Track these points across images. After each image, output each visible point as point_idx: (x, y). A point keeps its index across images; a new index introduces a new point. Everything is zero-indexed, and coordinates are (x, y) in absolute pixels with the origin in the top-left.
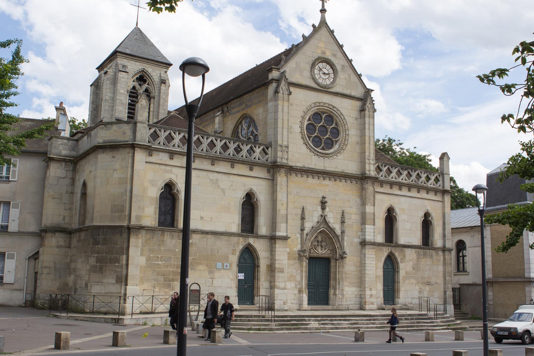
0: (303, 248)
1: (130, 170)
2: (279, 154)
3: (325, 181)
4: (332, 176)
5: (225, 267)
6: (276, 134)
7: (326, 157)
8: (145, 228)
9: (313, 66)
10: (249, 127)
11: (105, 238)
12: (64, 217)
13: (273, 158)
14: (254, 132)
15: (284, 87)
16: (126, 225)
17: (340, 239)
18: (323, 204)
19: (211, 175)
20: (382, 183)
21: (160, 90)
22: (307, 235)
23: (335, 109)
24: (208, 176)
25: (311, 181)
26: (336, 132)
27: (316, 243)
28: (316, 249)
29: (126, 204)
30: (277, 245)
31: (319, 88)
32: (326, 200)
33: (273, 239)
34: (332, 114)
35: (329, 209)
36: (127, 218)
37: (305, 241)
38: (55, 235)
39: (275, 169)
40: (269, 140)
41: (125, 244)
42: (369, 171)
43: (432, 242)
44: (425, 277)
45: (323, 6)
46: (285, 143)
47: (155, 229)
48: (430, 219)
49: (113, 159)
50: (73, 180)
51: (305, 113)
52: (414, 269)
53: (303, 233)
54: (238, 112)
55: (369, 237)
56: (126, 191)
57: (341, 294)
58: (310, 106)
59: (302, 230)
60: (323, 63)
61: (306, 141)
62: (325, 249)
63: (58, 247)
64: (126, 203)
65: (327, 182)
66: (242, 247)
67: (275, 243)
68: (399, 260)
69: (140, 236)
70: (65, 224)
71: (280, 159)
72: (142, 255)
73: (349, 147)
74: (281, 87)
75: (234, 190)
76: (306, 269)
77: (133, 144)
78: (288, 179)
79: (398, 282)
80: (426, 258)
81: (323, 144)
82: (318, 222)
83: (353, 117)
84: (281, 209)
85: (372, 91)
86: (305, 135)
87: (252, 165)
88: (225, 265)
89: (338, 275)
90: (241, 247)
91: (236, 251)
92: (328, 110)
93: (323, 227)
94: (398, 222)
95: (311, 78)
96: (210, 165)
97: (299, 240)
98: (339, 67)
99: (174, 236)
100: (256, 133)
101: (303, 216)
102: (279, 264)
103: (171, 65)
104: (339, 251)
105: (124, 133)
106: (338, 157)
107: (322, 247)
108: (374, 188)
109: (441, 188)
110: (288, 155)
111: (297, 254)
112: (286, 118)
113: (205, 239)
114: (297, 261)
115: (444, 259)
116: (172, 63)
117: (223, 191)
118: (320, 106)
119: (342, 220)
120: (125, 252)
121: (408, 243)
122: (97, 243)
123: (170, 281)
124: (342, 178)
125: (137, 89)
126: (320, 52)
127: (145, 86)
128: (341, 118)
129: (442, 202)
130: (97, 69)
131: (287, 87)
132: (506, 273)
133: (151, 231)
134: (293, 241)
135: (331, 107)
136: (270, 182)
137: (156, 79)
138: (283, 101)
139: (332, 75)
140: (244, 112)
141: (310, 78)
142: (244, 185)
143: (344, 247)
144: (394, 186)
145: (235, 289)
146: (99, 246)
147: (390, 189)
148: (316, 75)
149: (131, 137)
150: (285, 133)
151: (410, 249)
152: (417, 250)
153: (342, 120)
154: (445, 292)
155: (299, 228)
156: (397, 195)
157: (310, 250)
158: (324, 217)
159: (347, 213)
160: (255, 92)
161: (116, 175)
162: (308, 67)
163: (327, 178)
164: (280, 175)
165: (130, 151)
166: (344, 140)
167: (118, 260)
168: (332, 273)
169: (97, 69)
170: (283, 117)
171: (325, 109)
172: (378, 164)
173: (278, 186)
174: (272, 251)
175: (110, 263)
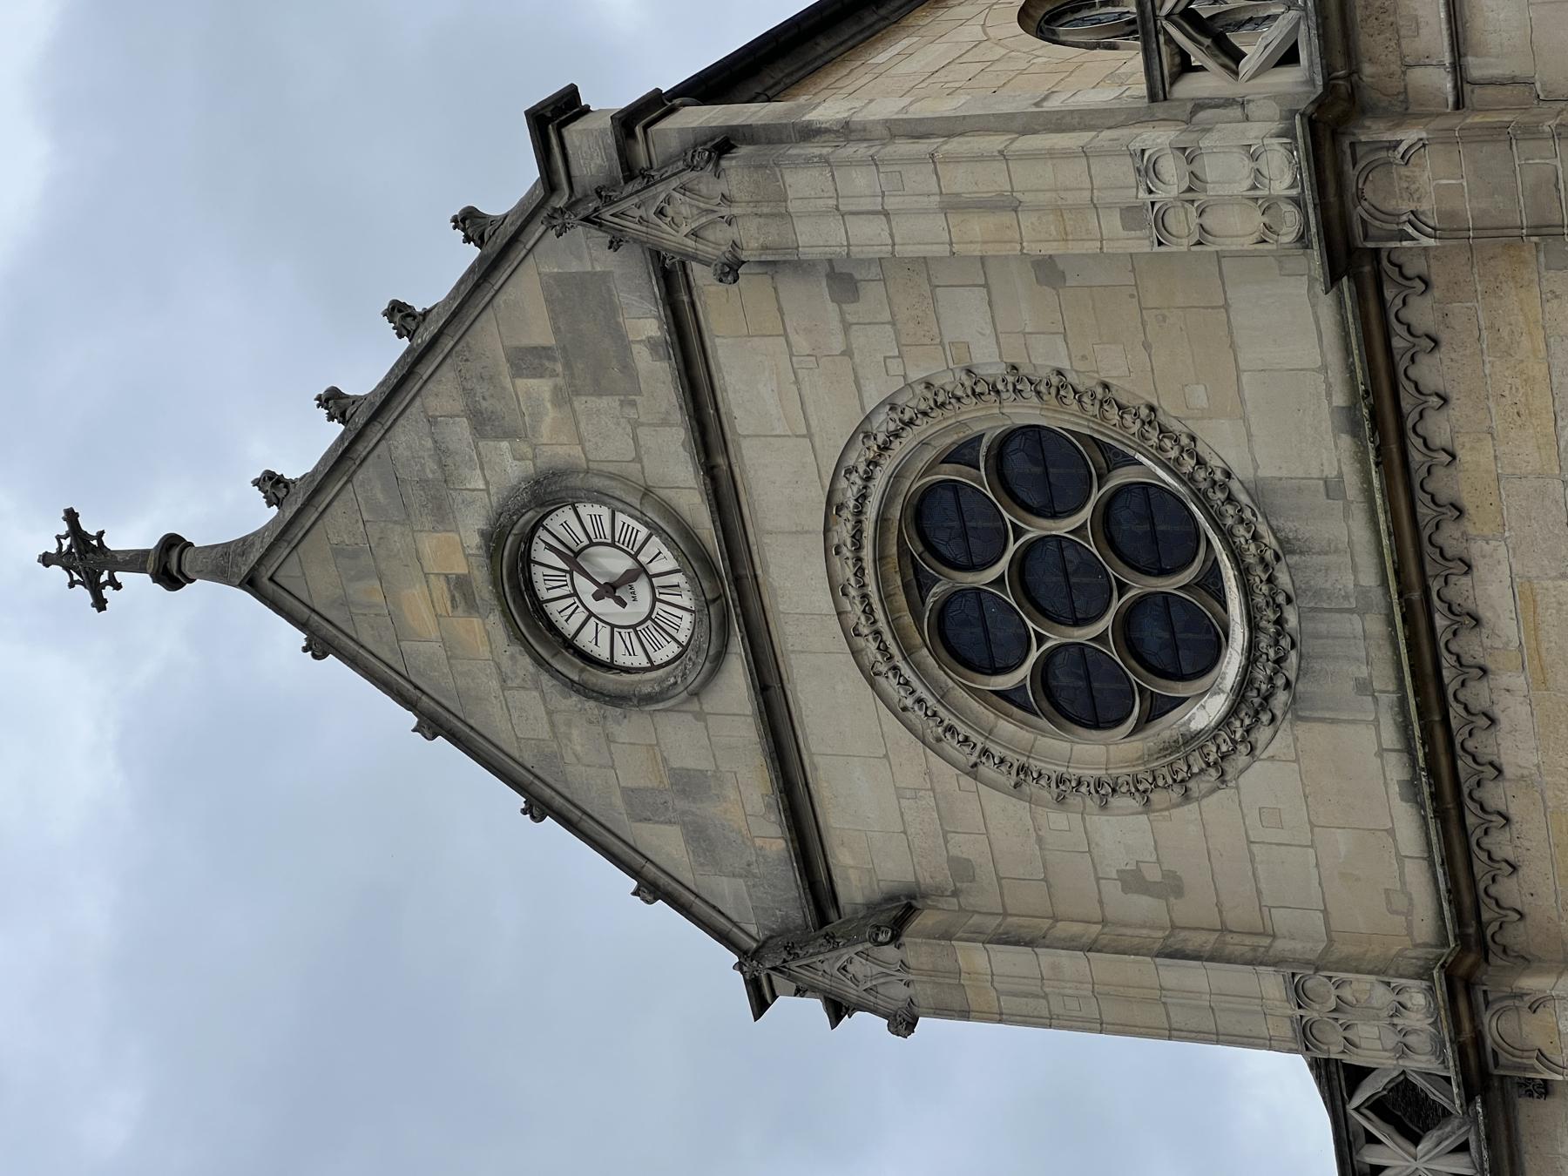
3: (1485, 613)
31: (737, 645)
34: (896, 512)
60: (544, 594)
83: (846, 327)
92: (880, 558)
95: (695, 706)
126: (476, 622)
135: (843, 532)
139: (596, 519)
141: (700, 716)
162: (630, 728)
171: (882, 581)
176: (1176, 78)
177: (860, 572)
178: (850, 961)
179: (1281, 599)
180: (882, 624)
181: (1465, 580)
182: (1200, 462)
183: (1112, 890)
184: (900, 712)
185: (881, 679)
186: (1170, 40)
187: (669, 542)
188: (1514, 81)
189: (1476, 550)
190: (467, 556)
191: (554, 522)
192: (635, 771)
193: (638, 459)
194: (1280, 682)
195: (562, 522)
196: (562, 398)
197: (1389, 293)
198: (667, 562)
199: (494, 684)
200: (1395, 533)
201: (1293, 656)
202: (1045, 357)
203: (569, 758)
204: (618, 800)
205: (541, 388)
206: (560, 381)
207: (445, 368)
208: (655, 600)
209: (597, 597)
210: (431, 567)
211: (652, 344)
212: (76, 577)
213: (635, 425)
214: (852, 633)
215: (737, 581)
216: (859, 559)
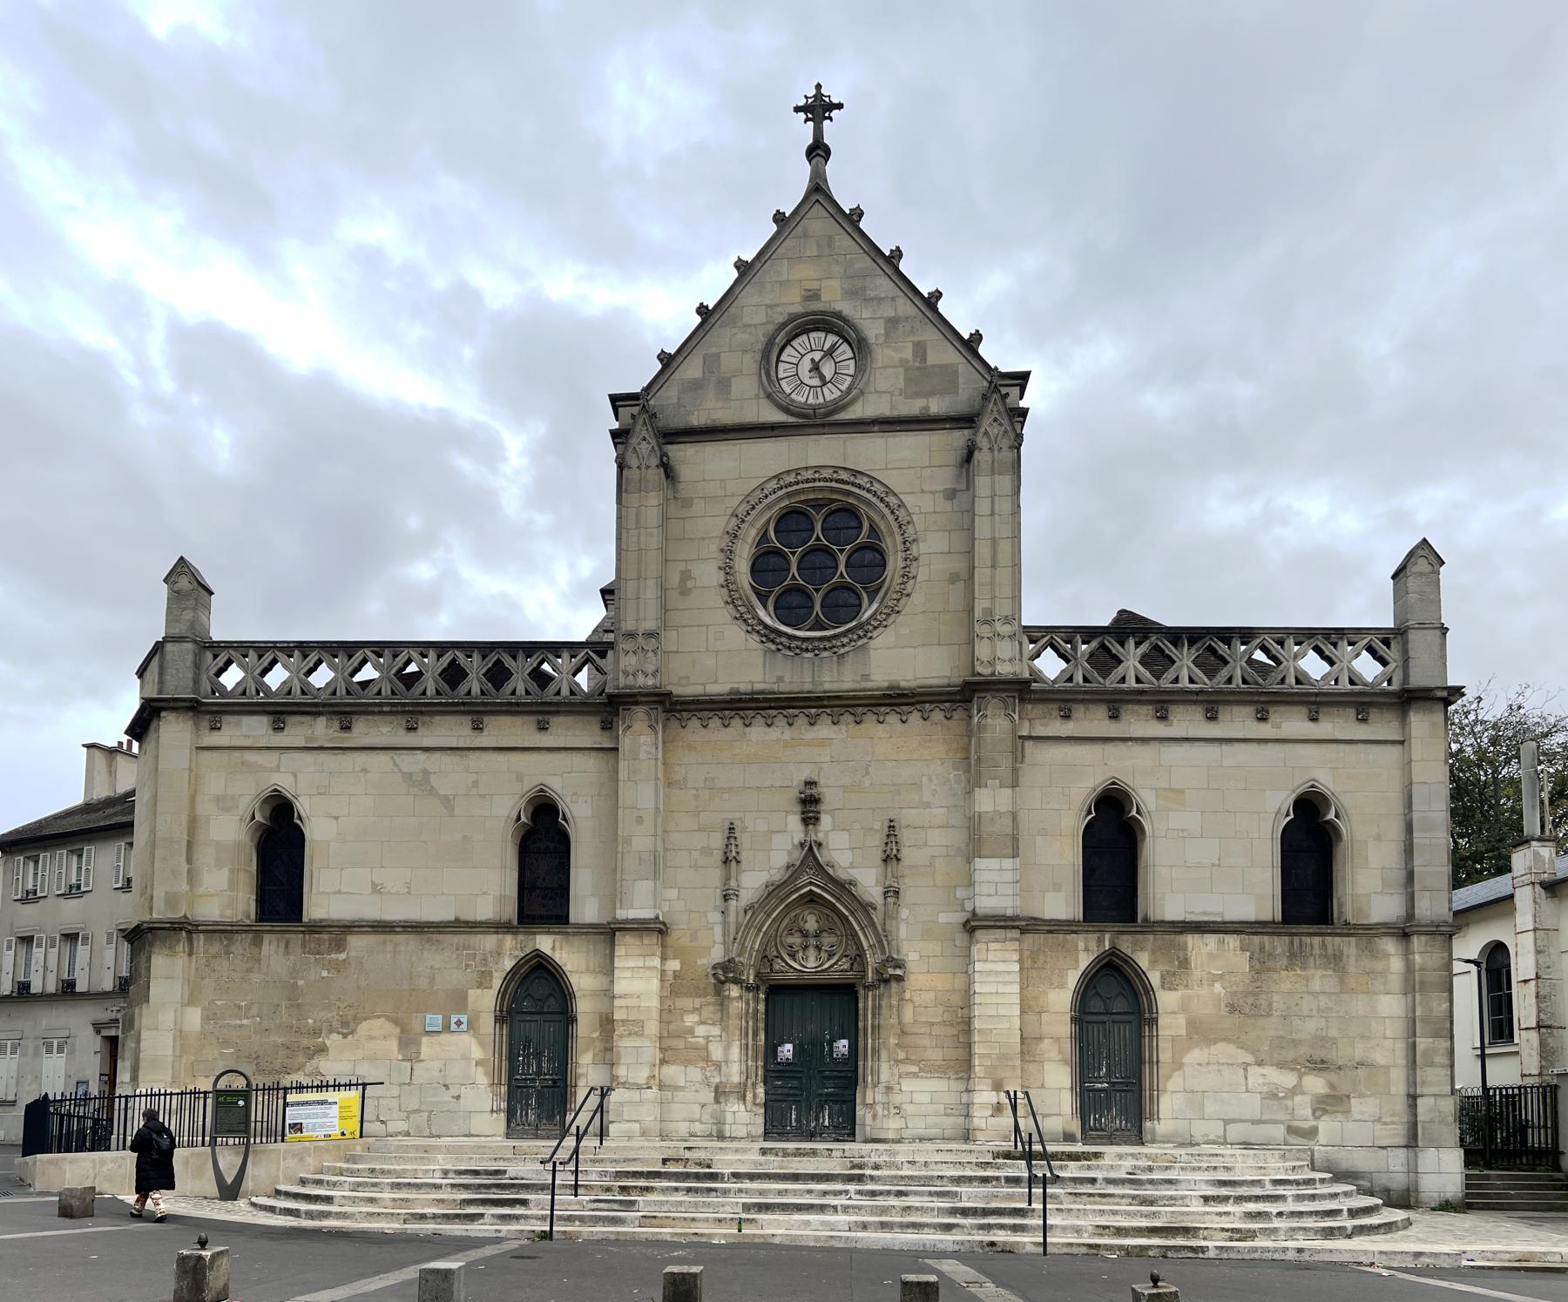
3: (815, 728)
4: (843, 710)
5: (453, 1027)
7: (825, 649)
8: (200, 928)
9: (770, 353)
18: (810, 805)
19: (407, 762)
23: (862, 481)
24: (396, 764)
25: (761, 735)
26: (871, 560)
28: (793, 956)
31: (792, 419)
34: (851, 500)
35: (834, 821)
48: (1331, 816)
52: (1233, 1008)
60: (812, 335)
62: (830, 956)
65: (824, 730)
66: (513, 963)
68: (1154, 978)
71: (631, 677)
73: (917, 600)
75: (484, 796)
80: (1303, 968)
82: (788, 867)
83: (933, 493)
90: (509, 964)
91: (491, 977)
92: (832, 490)
93: (811, 883)
95: (762, 395)
96: (402, 732)
97: (718, 930)
99: (291, 946)
104: (872, 960)
107: (818, 948)
111: (710, 976)
113: (389, 948)
114: (711, 999)
115: (1409, 968)
117: (447, 801)
119: (885, 851)
121: (1205, 913)
126: (799, 300)
129: (1402, 742)
133: (223, 936)
135: (844, 476)
141: (757, 397)
142: (520, 778)
144: (1125, 707)
147: (1107, 721)
148: (783, 383)
151: (1212, 940)
152: (1256, 939)
153: (893, 513)
156: (1145, 740)
158: (811, 848)
162: (750, 363)
163: (824, 716)
164: (629, 727)
171: (821, 489)
176: (1029, 637)
177: (826, 480)
178: (649, 443)
179: (817, 652)
180: (801, 486)
181: (830, 722)
182: (875, 628)
183: (682, 566)
184: (761, 487)
185: (776, 481)
186: (1043, 637)
187: (841, 398)
188: (1023, 756)
189: (843, 727)
190: (830, 302)
191: (845, 347)
192: (728, 362)
193: (876, 392)
194: (780, 647)
195: (845, 351)
196: (903, 362)
197: (947, 705)
198: (829, 397)
199: (768, 302)
200: (855, 698)
201: (792, 654)
202: (922, 573)
203: (734, 331)
204: (714, 350)
205: (908, 354)
206: (911, 363)
207: (918, 310)
208: (811, 387)
209: (812, 360)
210: (825, 283)
211: (927, 408)
212: (810, 101)
213: (892, 394)
214: (797, 472)
215: (823, 425)
216: (831, 481)
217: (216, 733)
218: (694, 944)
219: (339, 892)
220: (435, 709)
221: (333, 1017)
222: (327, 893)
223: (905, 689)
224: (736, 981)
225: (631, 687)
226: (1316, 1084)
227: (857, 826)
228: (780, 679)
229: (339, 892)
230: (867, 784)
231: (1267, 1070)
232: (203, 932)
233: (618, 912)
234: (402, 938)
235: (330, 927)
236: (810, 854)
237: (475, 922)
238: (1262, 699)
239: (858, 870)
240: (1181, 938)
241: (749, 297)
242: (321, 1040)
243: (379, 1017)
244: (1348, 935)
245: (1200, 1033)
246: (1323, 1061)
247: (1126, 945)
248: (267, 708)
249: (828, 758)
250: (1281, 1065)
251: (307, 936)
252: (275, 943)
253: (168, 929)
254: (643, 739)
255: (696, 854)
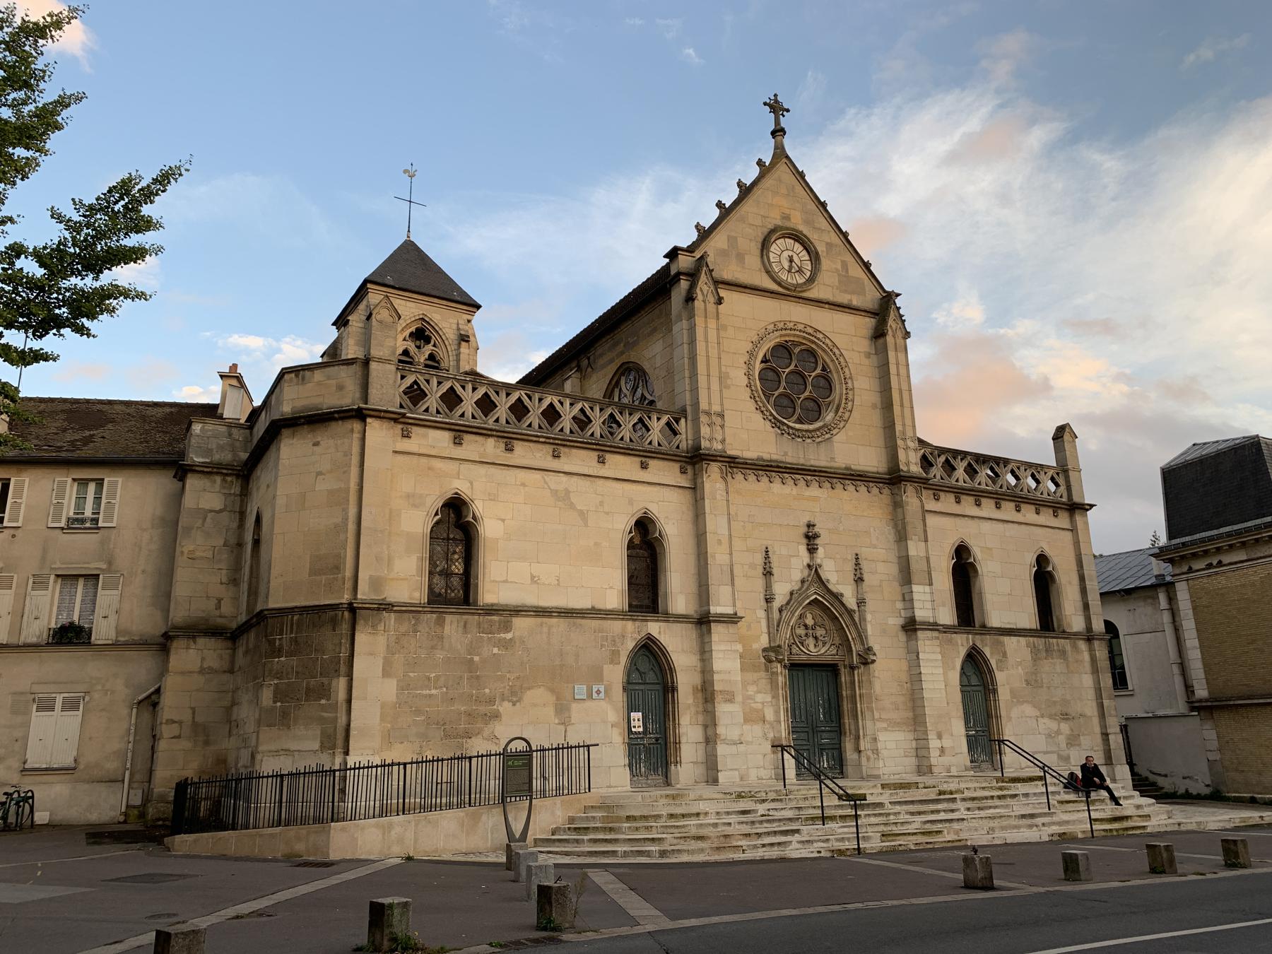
0: (775, 642)
1: (354, 471)
2: (705, 431)
3: (810, 489)
5: (595, 695)
6: (695, 390)
8: (395, 608)
9: (765, 245)
10: (636, 390)
11: (296, 637)
12: (219, 601)
13: (690, 442)
14: (645, 398)
15: (705, 288)
16: (344, 601)
17: (857, 619)
18: (811, 538)
19: (552, 479)
20: (937, 490)
21: (458, 355)
22: (780, 611)
23: (821, 336)
25: (780, 490)
27: (801, 631)
29: (346, 551)
30: (715, 637)
31: (780, 290)
32: (816, 529)
33: (703, 621)
34: (813, 346)
36: (348, 585)
37: (778, 626)
38: (195, 643)
39: (697, 466)
40: (677, 406)
41: (343, 649)
42: (908, 464)
43: (1059, 620)
44: (1055, 702)
45: (777, 122)
46: (716, 408)
47: (421, 609)
48: (1050, 569)
49: (316, 448)
50: (242, 515)
51: (756, 345)
52: (1028, 683)
53: (772, 608)
54: (612, 361)
55: (922, 614)
56: (346, 519)
57: (872, 750)
58: (764, 330)
59: (769, 600)
61: (761, 405)
62: (824, 644)
63: (202, 671)
64: (346, 549)
65: (814, 491)
67: (709, 631)
68: (993, 663)
69: (381, 627)
70: (220, 617)
72: (386, 673)
74: (698, 288)
75: (607, 513)
76: (786, 692)
77: (360, 410)
78: (727, 486)
79: (998, 717)
80: (1052, 658)
81: (798, 410)
82: (803, 582)
84: (718, 556)
85: (898, 295)
86: (757, 391)
87: (646, 455)
88: (595, 690)
89: (861, 704)
90: (630, 645)
91: (619, 654)
92: (804, 338)
94: (980, 577)
96: (550, 458)
97: (764, 623)
98: (821, 248)
99: (468, 626)
100: (651, 398)
101: (768, 569)
102: (722, 680)
103: (478, 307)
105: (340, 388)
106: (836, 438)
107: (816, 638)
108: (921, 501)
109: (1064, 499)
110: (724, 433)
112: (713, 353)
114: (763, 674)
116: (479, 302)
117: (583, 515)
118: (786, 329)
119: (855, 575)
120: (343, 669)
122: (278, 652)
123: (463, 737)
124: (847, 482)
125: (412, 353)
127: (428, 349)
128: (834, 354)
130: (333, 324)
131: (712, 287)
132: (1246, 685)
134: (749, 627)
136: (688, 494)
137: (450, 334)
138: (706, 317)
140: (624, 359)
141: (760, 270)
142: (631, 502)
143: (866, 638)
145: (622, 747)
146: (282, 659)
148: (773, 264)
149: (358, 395)
150: (715, 386)
151: (1014, 639)
152: (1031, 639)
154: (1105, 735)
155: (762, 596)
156: (973, 517)
157: (790, 646)
158: (816, 569)
159: (866, 559)
160: (643, 312)
161: (323, 485)
162: (755, 248)
164: (709, 476)
165: (355, 425)
166: (844, 401)
167: (324, 691)
168: (845, 699)
169: (333, 324)
170: (707, 352)
172: (923, 451)
173: (707, 502)
174: (704, 653)
175: (306, 700)
197: (881, 485)
199: (762, 213)
211: (851, 300)
217: (406, 440)
218: (749, 633)
219: (506, 581)
220: (576, 444)
221: (505, 687)
222: (496, 582)
223: (854, 471)
224: (780, 661)
225: (708, 449)
226: (1065, 727)
227: (838, 556)
228: (786, 454)
229: (506, 581)
230: (841, 528)
231: (1046, 720)
232: (395, 611)
233: (711, 608)
234: (554, 621)
235: (504, 610)
236: (814, 571)
237: (605, 611)
238: (1020, 500)
239: (841, 586)
240: (1002, 638)
241: (748, 207)
242: (495, 707)
243: (540, 686)
244: (1066, 638)
245: (1017, 697)
246: (1066, 714)
247: (979, 645)
248: (453, 427)
249: (818, 510)
250: (1051, 717)
251: (481, 617)
252: (455, 624)
253: (373, 609)
254: (718, 485)
255: (746, 567)
